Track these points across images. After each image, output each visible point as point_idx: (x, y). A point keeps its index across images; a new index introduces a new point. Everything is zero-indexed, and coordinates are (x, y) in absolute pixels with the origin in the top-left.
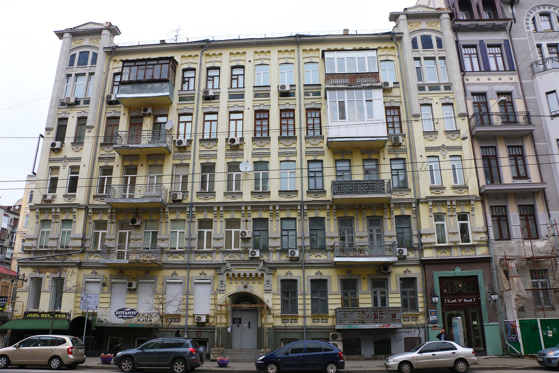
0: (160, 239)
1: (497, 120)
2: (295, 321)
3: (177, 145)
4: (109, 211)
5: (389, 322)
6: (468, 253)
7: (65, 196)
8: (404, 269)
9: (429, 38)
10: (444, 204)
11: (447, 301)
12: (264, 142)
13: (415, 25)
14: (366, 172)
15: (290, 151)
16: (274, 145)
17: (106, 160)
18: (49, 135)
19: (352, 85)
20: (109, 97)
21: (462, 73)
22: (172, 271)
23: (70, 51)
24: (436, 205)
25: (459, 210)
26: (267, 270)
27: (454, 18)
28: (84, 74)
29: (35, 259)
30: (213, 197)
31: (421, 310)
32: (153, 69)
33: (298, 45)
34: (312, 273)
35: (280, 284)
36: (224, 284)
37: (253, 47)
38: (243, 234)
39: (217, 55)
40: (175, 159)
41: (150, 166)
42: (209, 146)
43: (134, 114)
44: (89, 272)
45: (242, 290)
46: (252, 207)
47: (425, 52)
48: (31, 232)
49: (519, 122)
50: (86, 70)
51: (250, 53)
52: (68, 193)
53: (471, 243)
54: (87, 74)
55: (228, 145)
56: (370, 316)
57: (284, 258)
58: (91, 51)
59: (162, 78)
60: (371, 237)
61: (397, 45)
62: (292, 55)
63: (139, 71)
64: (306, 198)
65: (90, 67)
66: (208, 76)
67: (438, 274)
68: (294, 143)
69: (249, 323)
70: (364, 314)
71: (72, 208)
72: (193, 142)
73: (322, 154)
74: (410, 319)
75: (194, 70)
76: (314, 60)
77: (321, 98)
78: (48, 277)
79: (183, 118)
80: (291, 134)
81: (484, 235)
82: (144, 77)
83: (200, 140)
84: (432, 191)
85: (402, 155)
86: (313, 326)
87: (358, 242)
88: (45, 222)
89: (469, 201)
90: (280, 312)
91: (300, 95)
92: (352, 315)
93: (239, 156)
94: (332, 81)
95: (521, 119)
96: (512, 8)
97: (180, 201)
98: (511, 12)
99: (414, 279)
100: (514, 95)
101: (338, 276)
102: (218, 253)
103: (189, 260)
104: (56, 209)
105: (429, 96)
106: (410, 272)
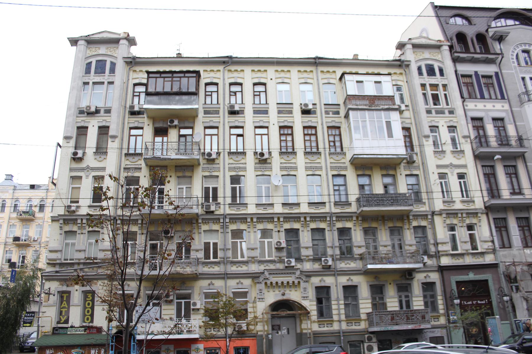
0: (193, 250)
1: (493, 142)
2: (331, 325)
3: (206, 157)
4: (140, 222)
5: (420, 323)
7: (90, 206)
8: (425, 274)
9: (432, 67)
10: (455, 216)
11: (464, 303)
12: (291, 157)
13: (419, 54)
14: (385, 187)
16: (300, 160)
17: (131, 171)
18: (68, 144)
20: (132, 107)
21: (463, 100)
22: (209, 281)
23: (85, 58)
24: (449, 217)
25: (468, 221)
26: (304, 278)
27: (453, 49)
28: (103, 83)
30: (245, 208)
31: (442, 312)
32: (180, 81)
33: (317, 66)
34: (343, 280)
36: (263, 293)
37: (274, 65)
38: (279, 244)
39: (239, 71)
40: (204, 170)
41: (178, 177)
42: (237, 159)
43: (159, 125)
45: (280, 298)
46: (284, 218)
47: (430, 80)
48: (55, 245)
49: (511, 145)
50: (104, 79)
51: (271, 70)
52: (93, 202)
53: (479, 251)
54: (106, 83)
55: (257, 158)
57: (317, 266)
58: (109, 60)
59: (190, 91)
60: (393, 246)
61: (405, 72)
62: (311, 75)
63: (165, 82)
64: (334, 210)
65: (109, 76)
66: (230, 92)
67: (455, 278)
68: (318, 158)
70: (398, 317)
72: (222, 155)
73: (345, 169)
74: (433, 320)
75: (216, 84)
76: (332, 81)
77: (340, 117)
78: (77, 290)
79: (208, 131)
80: (314, 150)
81: (490, 244)
82: (172, 89)
83: (228, 153)
86: (348, 330)
87: (382, 250)
88: (70, 233)
89: (477, 213)
90: (316, 317)
91: (321, 113)
92: (387, 318)
93: (267, 170)
94: (354, 102)
95: (513, 143)
96: (500, 44)
97: (213, 212)
98: (499, 47)
99: (433, 284)
100: (506, 121)
101: (368, 282)
103: (225, 270)
105: (436, 119)
106: (429, 277)
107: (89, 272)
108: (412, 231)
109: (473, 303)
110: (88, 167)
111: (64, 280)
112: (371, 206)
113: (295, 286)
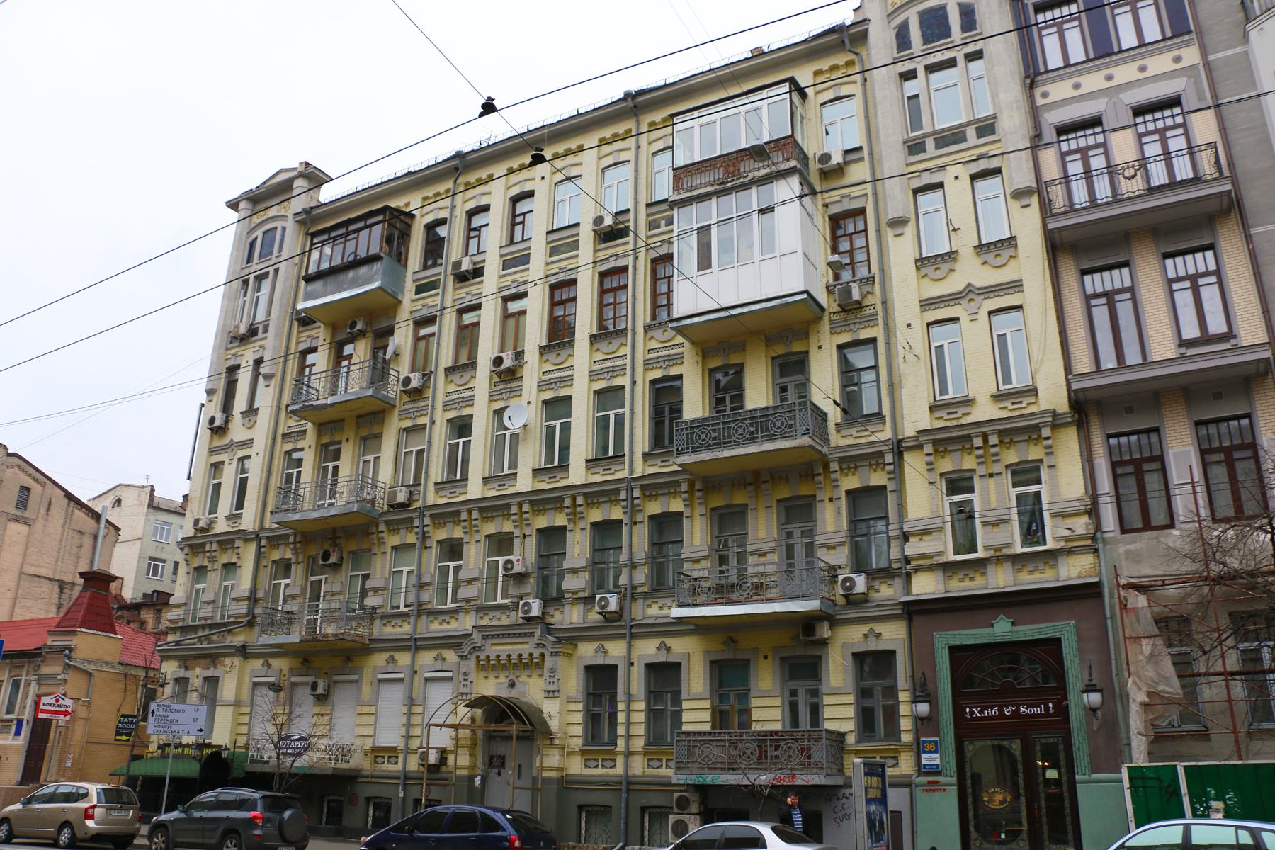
2: (612, 764)
6: (1037, 576)
8: (864, 629)
11: (972, 713)
15: (610, 365)
16: (582, 355)
19: (728, 182)
22: (385, 656)
25: (1011, 456)
34: (648, 649)
35: (582, 677)
44: (257, 664)
45: (504, 693)
56: (748, 752)
67: (945, 639)
69: (520, 766)
70: (736, 748)
71: (232, 541)
84: (938, 414)
85: (869, 329)
86: (648, 776)
89: (1037, 428)
101: (706, 653)
102: (467, 611)
108: (843, 503)
109: (1001, 711)
112: (698, 449)
113: (532, 665)
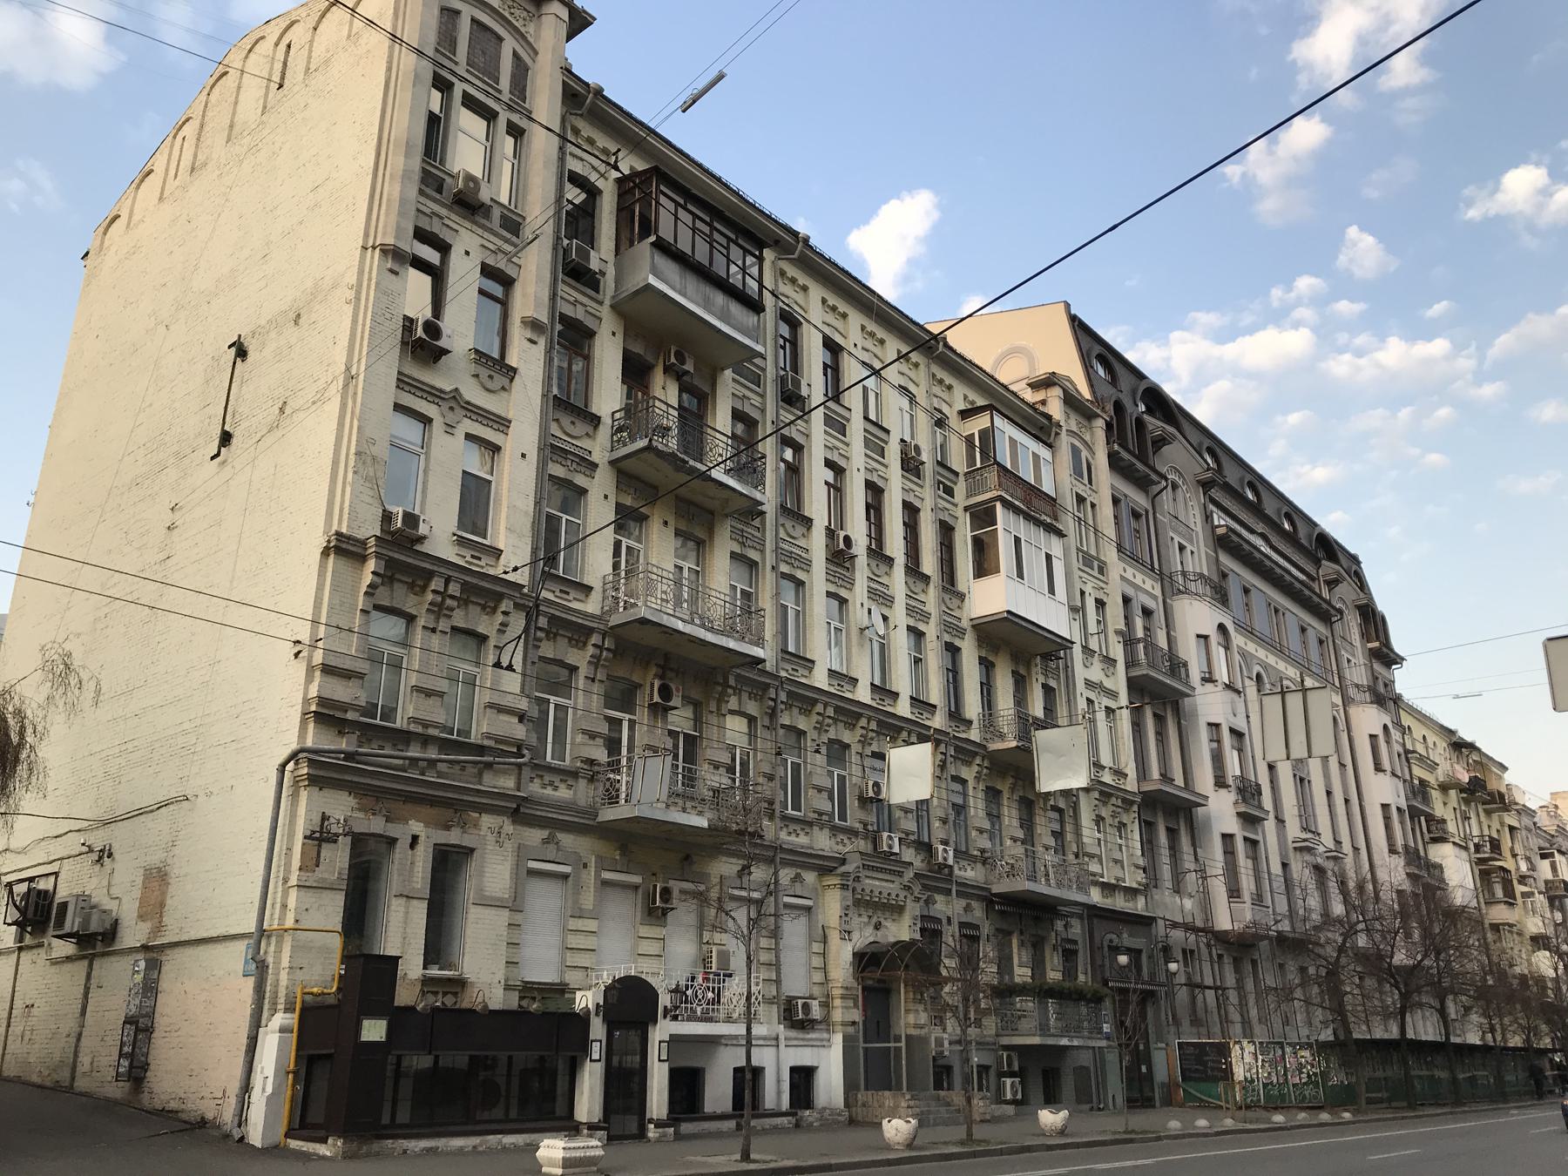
29: (363, 758)
104: (448, 581)
107: (451, 775)
110: (455, 395)
111: (372, 794)
